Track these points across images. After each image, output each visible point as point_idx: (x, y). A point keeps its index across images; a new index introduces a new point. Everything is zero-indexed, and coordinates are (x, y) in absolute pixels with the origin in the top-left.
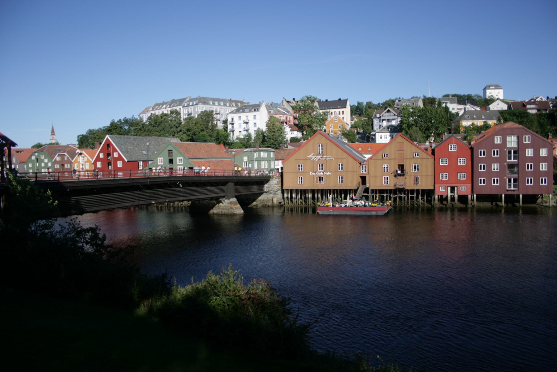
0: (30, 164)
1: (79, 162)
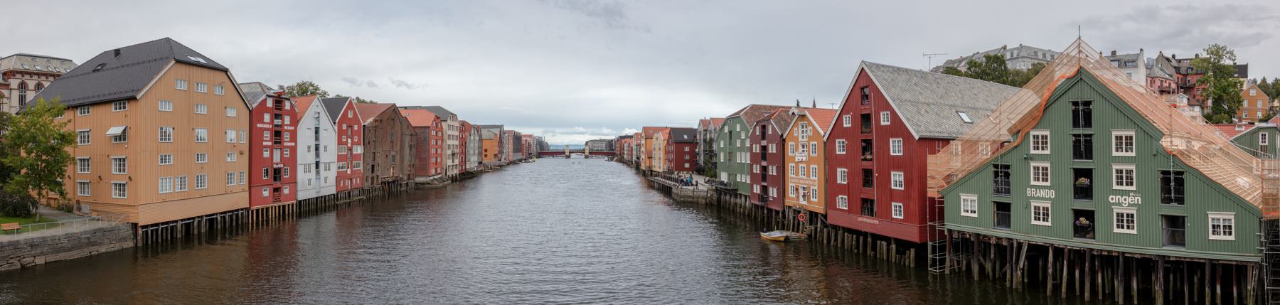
1: (797, 138)
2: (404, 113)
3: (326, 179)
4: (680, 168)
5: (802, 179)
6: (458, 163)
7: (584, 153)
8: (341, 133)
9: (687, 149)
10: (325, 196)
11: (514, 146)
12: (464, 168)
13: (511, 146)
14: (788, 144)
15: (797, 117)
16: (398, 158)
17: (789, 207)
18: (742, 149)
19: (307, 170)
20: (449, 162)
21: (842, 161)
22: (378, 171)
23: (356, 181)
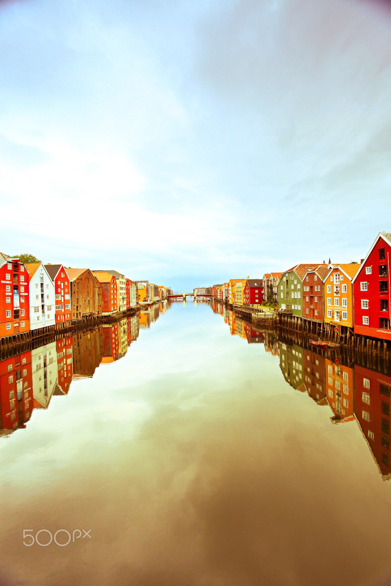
0: (281, 286)
1: (333, 282)
2: (94, 275)
3: (48, 316)
4: (253, 302)
5: (336, 307)
6: (126, 304)
7: (194, 295)
8: (57, 287)
9: (257, 291)
10: (49, 327)
11: (154, 293)
12: (129, 306)
13: (153, 293)
14: (326, 287)
15: (332, 270)
16: (91, 302)
17: (327, 323)
18: (295, 290)
19: (36, 310)
20: (121, 303)
21: (364, 295)
22: (81, 310)
23: (67, 316)
